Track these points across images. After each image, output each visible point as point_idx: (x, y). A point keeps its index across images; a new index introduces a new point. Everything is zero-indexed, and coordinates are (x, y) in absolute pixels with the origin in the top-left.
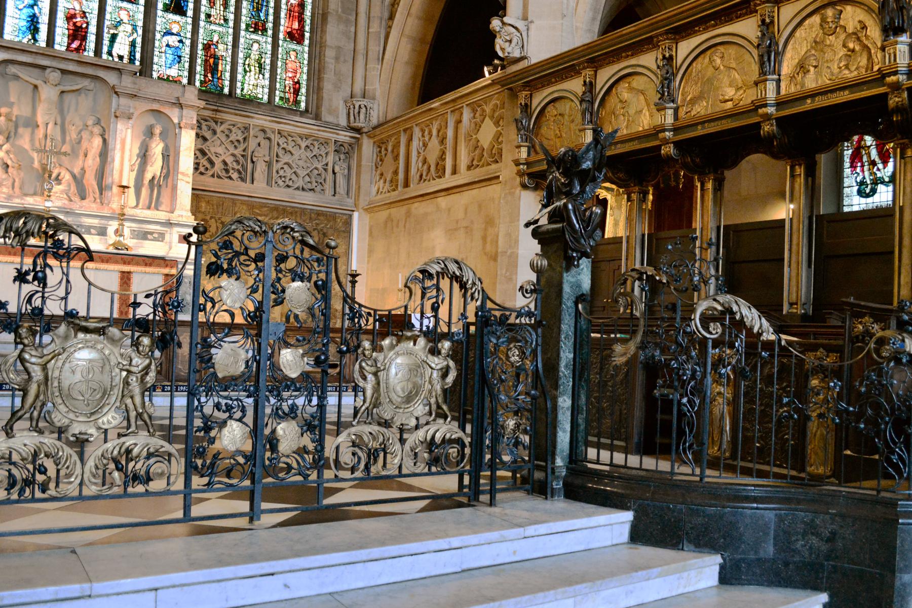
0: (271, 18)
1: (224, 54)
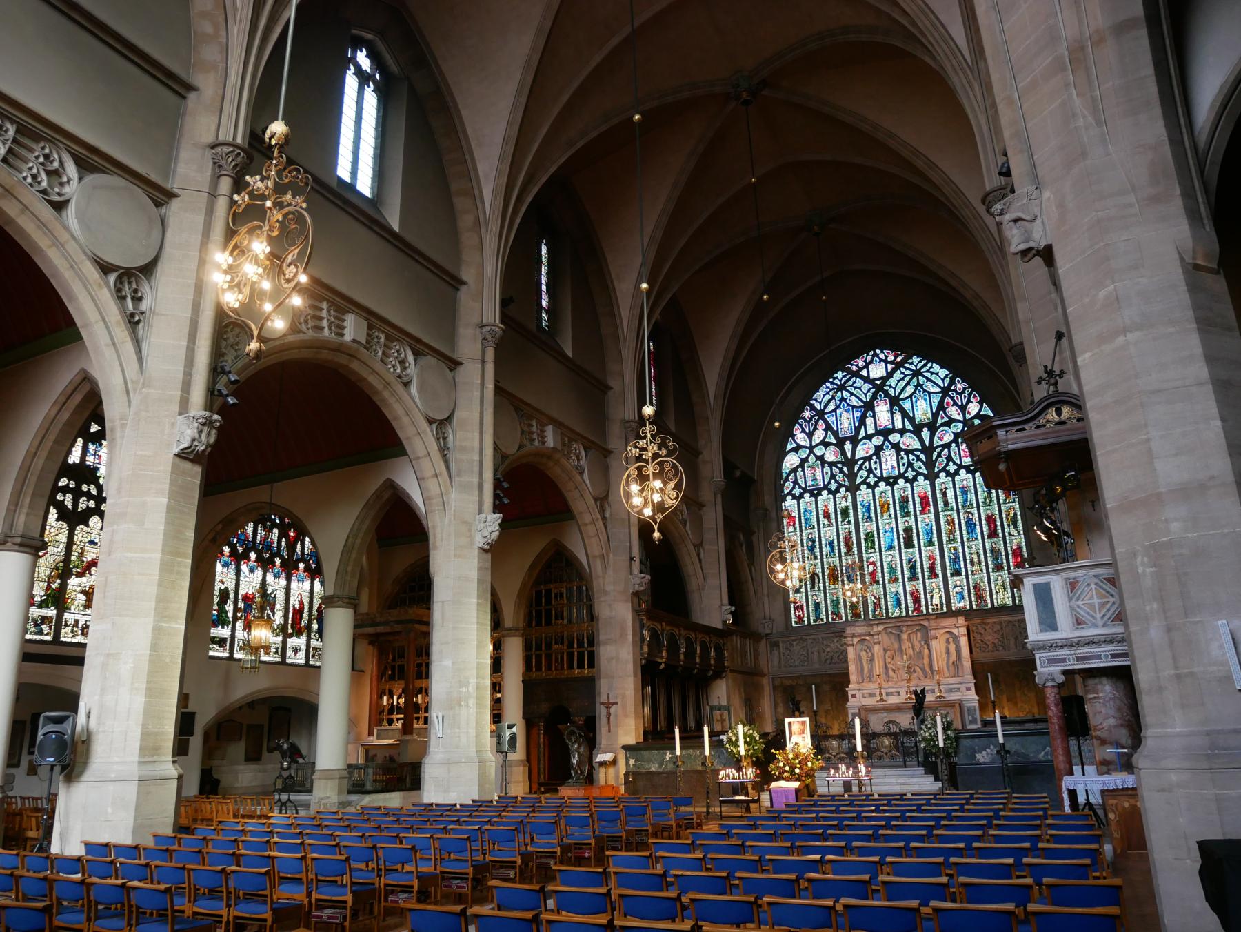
0: (1004, 561)
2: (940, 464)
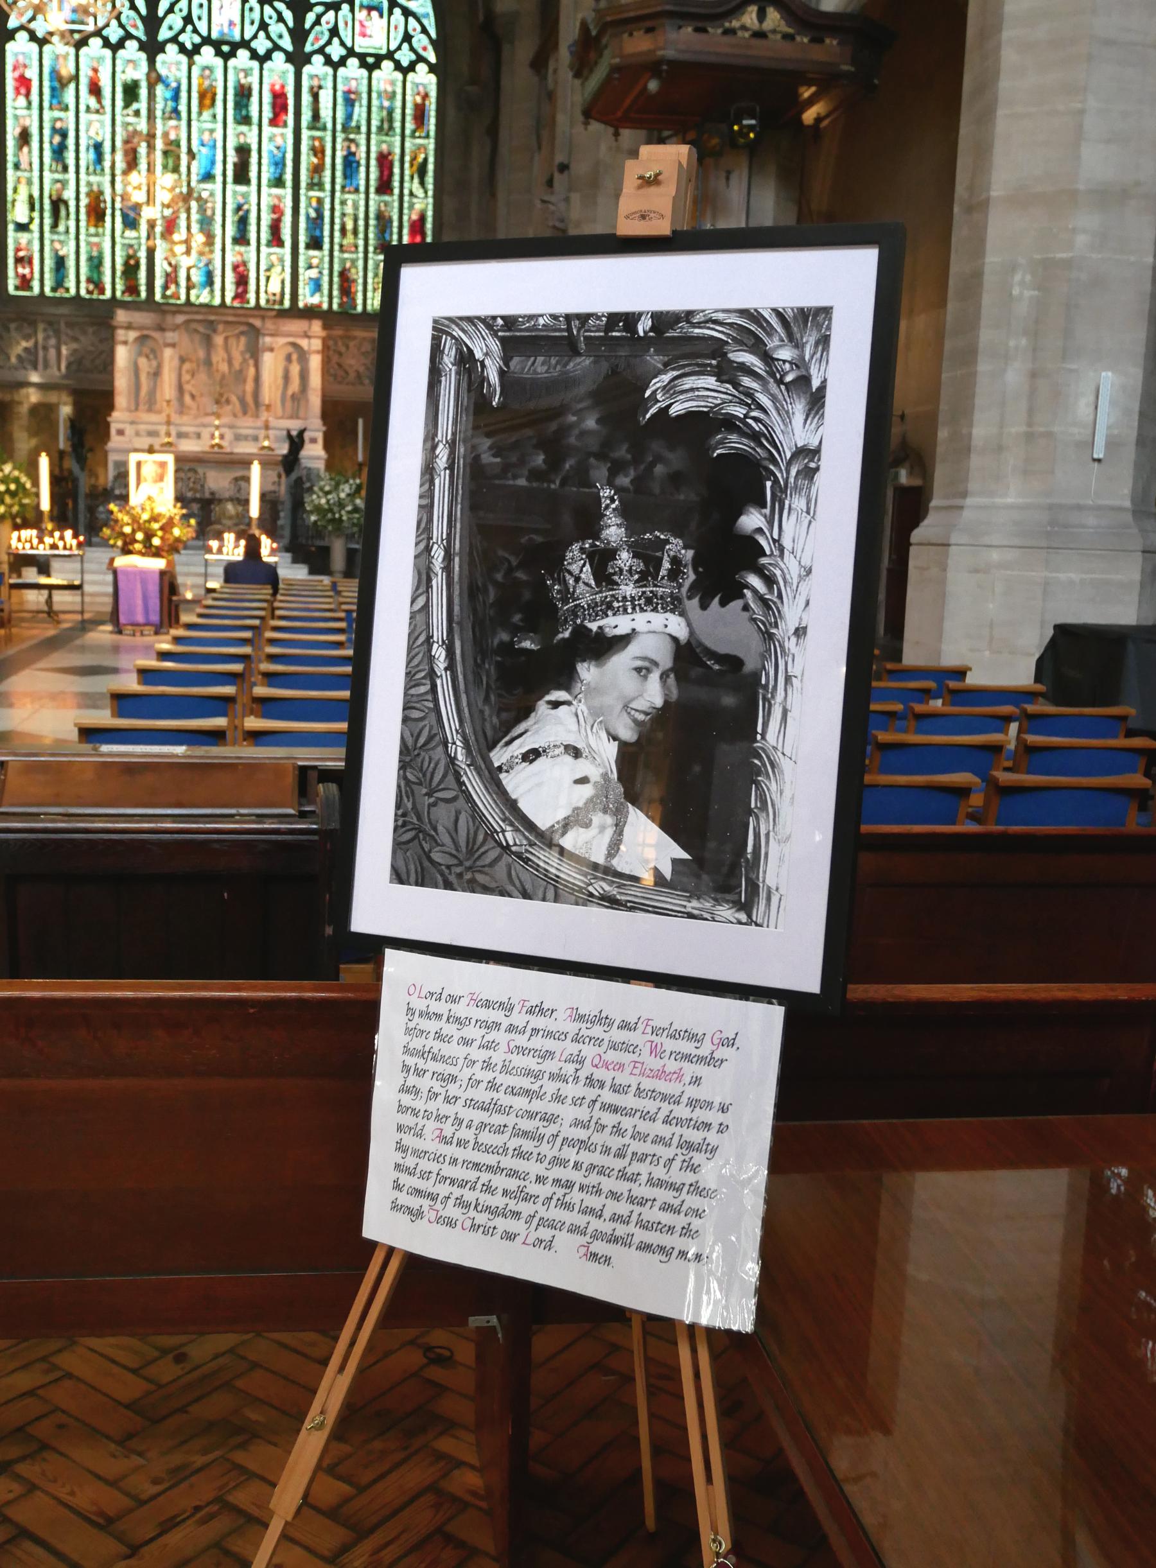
1: (355, 277)
2: (317, 39)
